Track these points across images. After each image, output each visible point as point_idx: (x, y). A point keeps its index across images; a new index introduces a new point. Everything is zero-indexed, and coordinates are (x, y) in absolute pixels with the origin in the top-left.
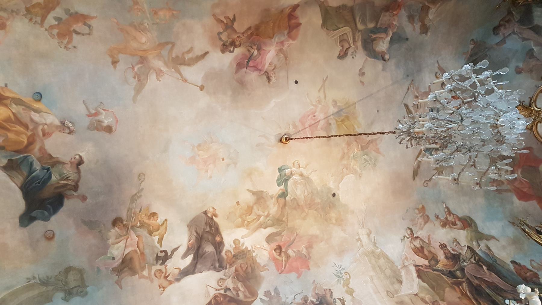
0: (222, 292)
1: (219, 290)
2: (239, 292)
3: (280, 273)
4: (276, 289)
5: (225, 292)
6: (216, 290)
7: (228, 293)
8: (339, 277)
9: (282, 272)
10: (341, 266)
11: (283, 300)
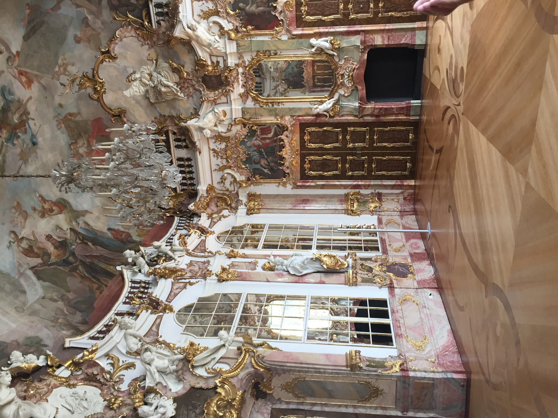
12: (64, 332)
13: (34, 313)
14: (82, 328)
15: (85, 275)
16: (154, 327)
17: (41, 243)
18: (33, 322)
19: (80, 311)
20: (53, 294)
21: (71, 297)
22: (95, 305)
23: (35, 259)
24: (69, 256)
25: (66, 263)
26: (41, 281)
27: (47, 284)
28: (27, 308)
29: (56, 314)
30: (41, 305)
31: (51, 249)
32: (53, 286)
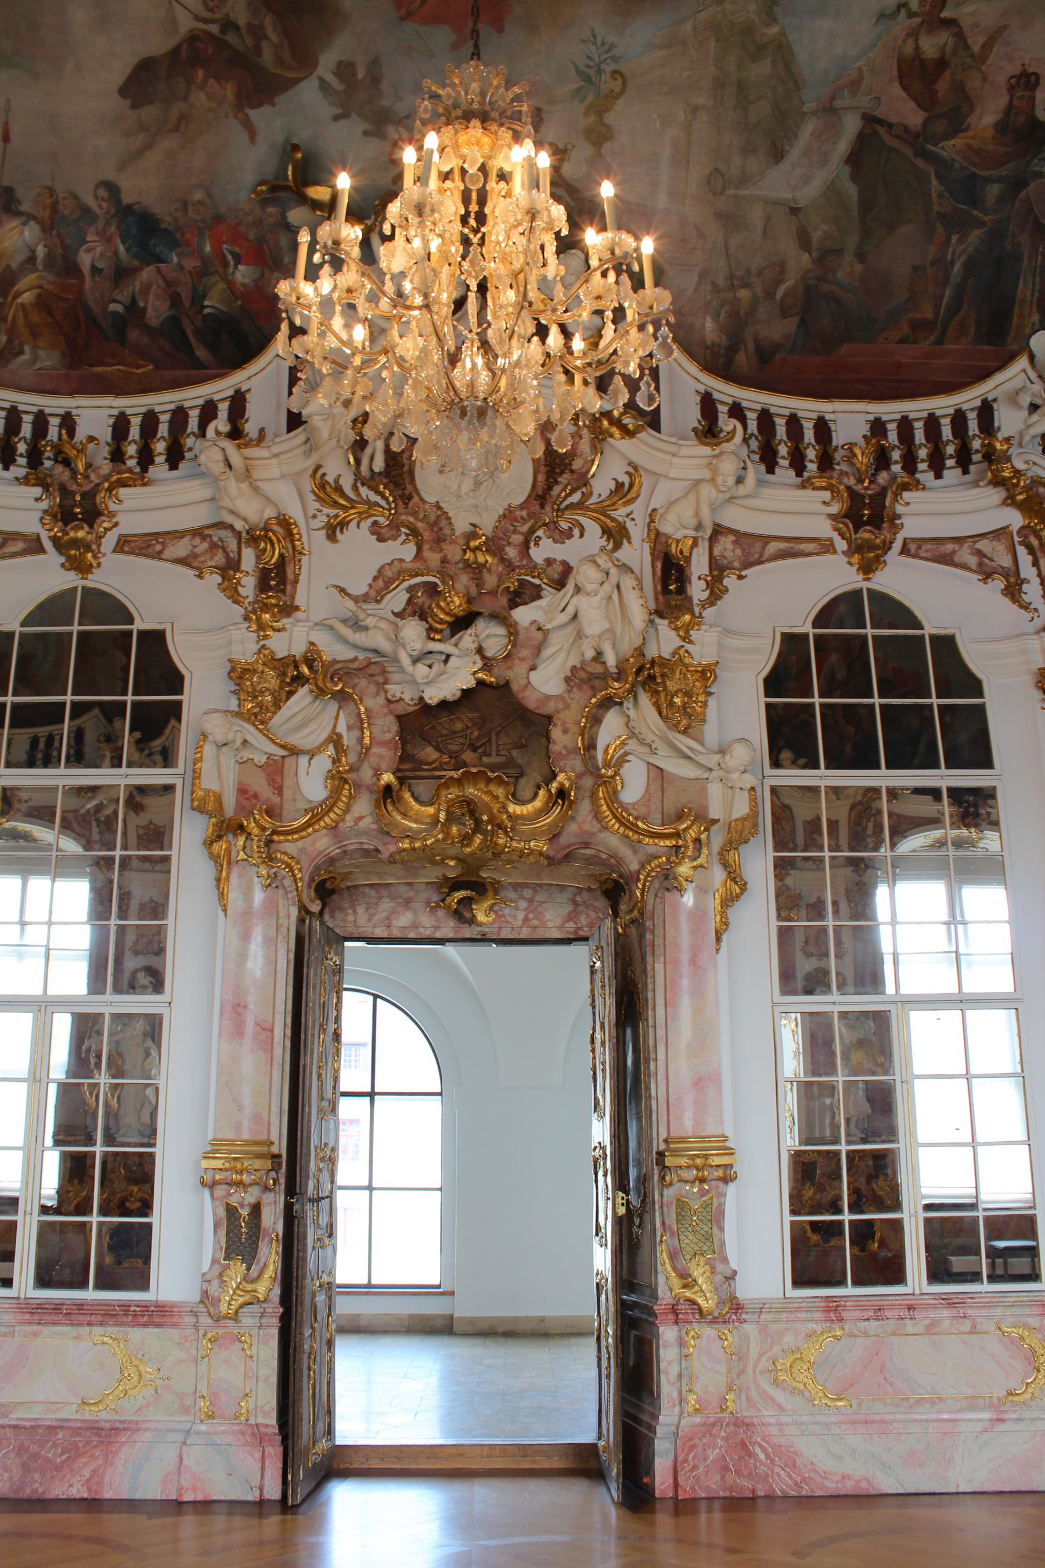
0: (214, 29)
1: (206, 21)
2: (264, 44)
3: (402, 19)
4: (375, 64)
5: (223, 31)
6: (197, 18)
7: (231, 38)
8: (588, 79)
9: (408, 16)
10: (613, 46)
11: (385, 103)
12: (709, 324)
13: (730, 220)
14: (743, 360)
15: (953, 262)
16: (782, 545)
17: (985, 79)
18: (701, 235)
19: (803, 323)
20: (825, 227)
21: (840, 275)
22: (845, 348)
23: (912, 105)
24: (999, 180)
25: (969, 189)
26: (847, 170)
27: (852, 191)
28: (736, 197)
29: (760, 274)
30: (768, 220)
31: (986, 118)
32: (855, 210)
